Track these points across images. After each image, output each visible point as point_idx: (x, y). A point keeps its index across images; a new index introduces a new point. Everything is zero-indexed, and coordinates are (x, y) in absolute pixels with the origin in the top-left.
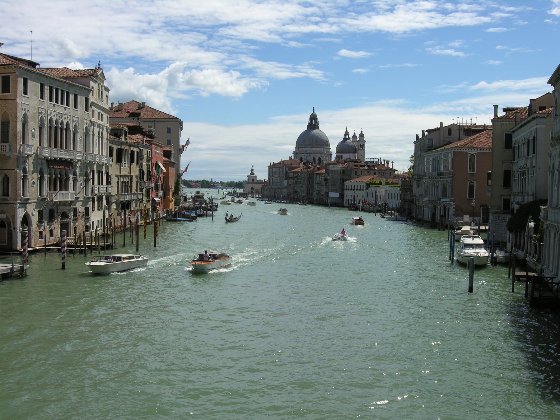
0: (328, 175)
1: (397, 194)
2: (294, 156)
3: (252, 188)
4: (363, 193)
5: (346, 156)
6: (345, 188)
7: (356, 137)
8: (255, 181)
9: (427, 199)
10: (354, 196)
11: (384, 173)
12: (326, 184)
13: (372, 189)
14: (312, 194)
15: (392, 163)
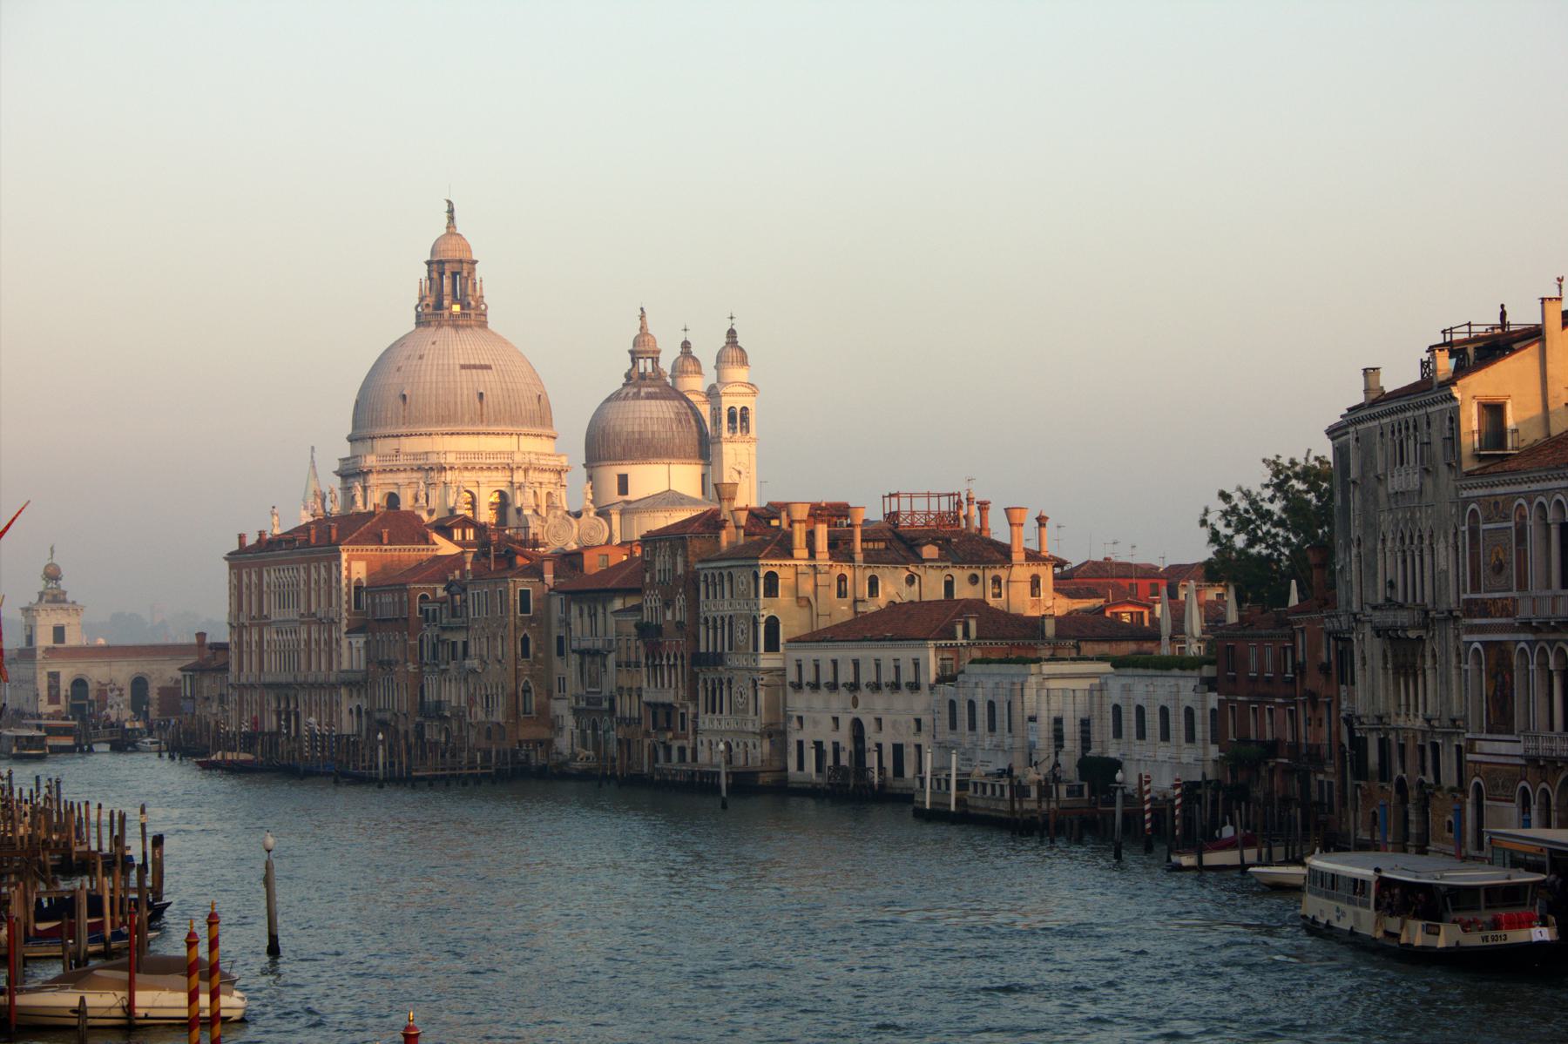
0: (668, 604)
1: (1189, 712)
2: (347, 490)
3: (79, 684)
4: (919, 704)
5: (648, 479)
6: (792, 676)
7: (699, 373)
8: (73, 639)
9: (1519, 749)
10: (857, 725)
11: (997, 581)
12: (654, 651)
13: (983, 684)
14: (544, 710)
15: (1041, 521)
